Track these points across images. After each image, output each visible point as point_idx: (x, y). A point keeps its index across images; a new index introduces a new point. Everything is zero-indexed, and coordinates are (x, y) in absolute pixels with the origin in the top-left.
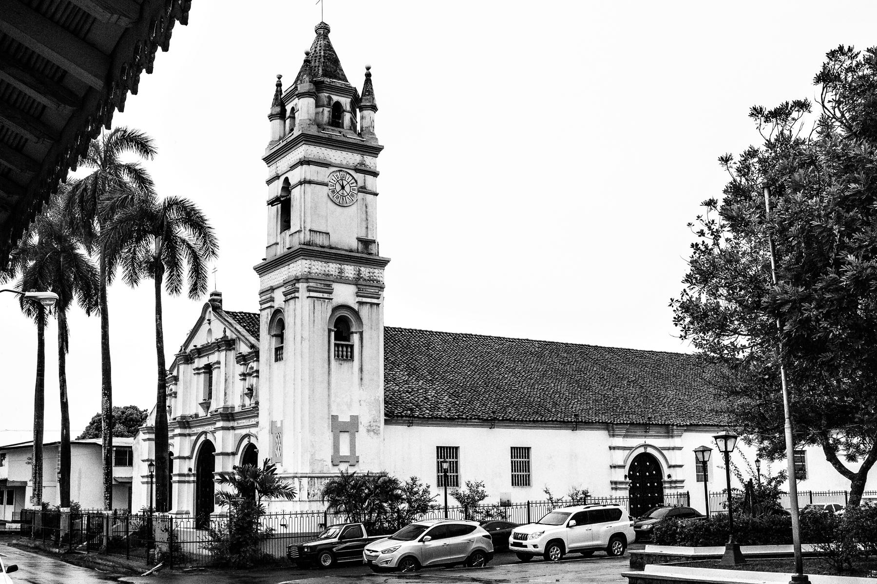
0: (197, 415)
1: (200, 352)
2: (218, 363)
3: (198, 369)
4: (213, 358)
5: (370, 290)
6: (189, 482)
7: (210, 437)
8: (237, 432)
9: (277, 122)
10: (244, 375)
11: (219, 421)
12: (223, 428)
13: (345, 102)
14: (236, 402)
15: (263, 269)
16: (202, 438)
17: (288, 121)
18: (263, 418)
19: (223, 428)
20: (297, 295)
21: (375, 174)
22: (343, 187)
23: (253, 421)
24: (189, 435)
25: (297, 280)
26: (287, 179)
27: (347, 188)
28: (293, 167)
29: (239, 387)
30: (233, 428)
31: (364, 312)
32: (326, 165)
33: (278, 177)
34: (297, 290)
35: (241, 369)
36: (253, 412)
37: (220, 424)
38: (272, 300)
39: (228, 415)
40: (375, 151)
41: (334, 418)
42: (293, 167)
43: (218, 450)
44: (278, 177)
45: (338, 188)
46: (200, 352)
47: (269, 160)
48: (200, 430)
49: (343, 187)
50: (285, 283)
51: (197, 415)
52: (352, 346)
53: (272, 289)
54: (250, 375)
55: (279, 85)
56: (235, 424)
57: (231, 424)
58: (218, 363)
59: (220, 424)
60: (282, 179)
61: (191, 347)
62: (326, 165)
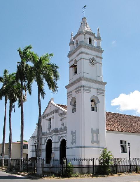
0: (46, 132)
1: (47, 115)
2: (53, 117)
3: (47, 120)
4: (51, 116)
5: (101, 92)
6: (44, 151)
7: (50, 138)
8: (59, 136)
9: (72, 45)
10: (61, 119)
11: (54, 133)
12: (55, 135)
13: (92, 38)
14: (59, 126)
15: (67, 87)
16: (48, 139)
17: (75, 45)
18: (69, 131)
19: (55, 135)
20: (80, 91)
21: (101, 58)
22: (93, 61)
23: (65, 132)
24: (44, 138)
25: (81, 87)
26: (76, 60)
27: (94, 61)
28: (77, 55)
29: (60, 123)
30: (58, 135)
31: (100, 97)
32: (88, 54)
33: (72, 60)
34: (80, 90)
35: (60, 117)
36: (65, 129)
37: (54, 134)
38: (71, 95)
39: (56, 131)
40: (102, 51)
41: (92, 129)
42: (77, 55)
43: (53, 141)
44: (72, 60)
45: (91, 61)
46: (47, 115)
47: (69, 56)
48: (47, 136)
49: (93, 61)
50: (76, 89)
51: (46, 132)
52: (96, 108)
53: (71, 92)
54: (63, 119)
55: (72, 36)
56: (58, 133)
57: (57, 134)
58: (53, 117)
59: (54, 134)
60: (74, 60)
61: (45, 114)
62: (88, 54)
